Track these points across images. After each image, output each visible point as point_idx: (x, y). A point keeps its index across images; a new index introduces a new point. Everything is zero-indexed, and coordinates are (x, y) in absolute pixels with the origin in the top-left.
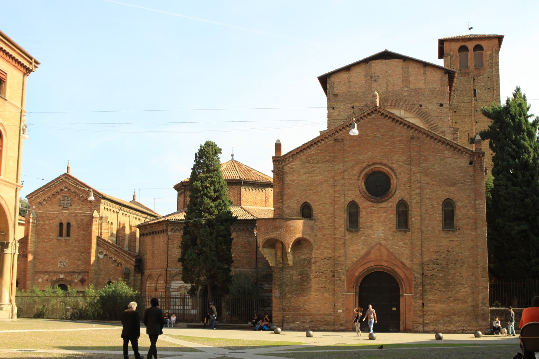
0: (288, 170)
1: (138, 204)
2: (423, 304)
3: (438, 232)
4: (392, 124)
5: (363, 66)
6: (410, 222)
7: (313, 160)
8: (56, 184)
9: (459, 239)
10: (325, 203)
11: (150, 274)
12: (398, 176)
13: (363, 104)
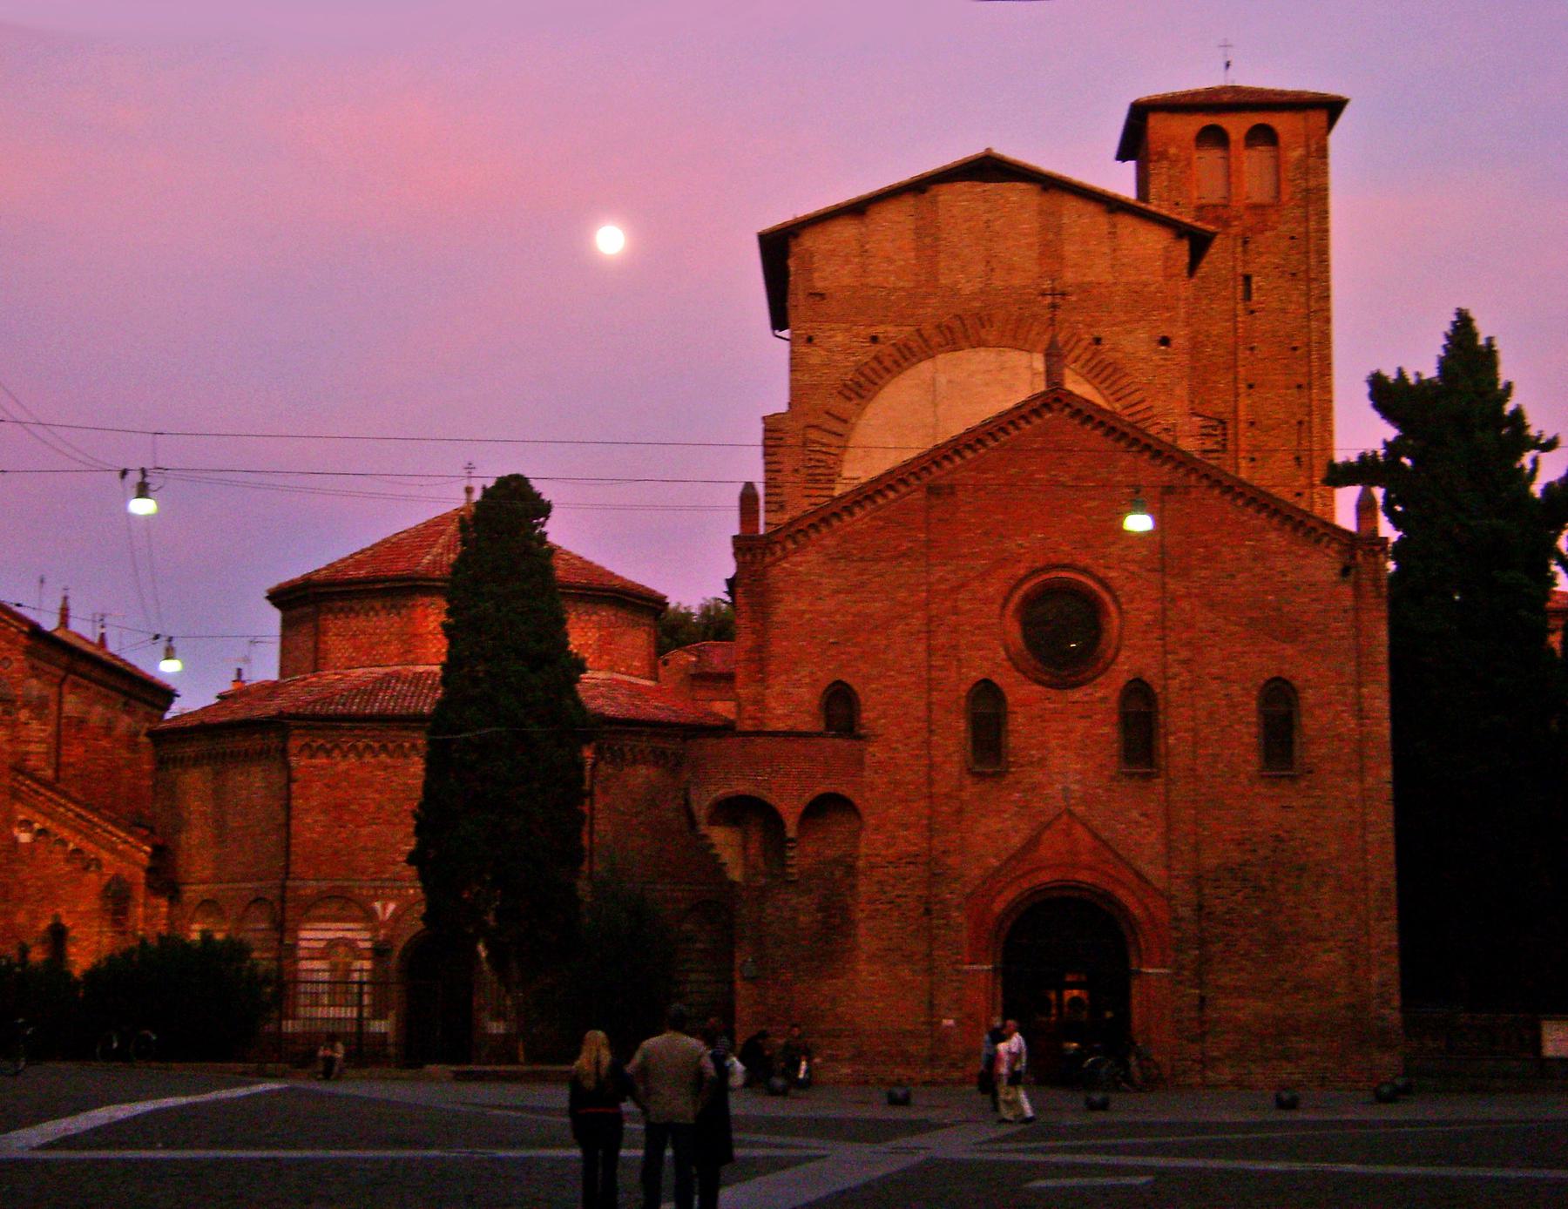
0: (783, 580)
3: (1246, 782)
6: (1163, 751)
9: (1312, 801)
12: (1124, 607)
13: (908, 328)
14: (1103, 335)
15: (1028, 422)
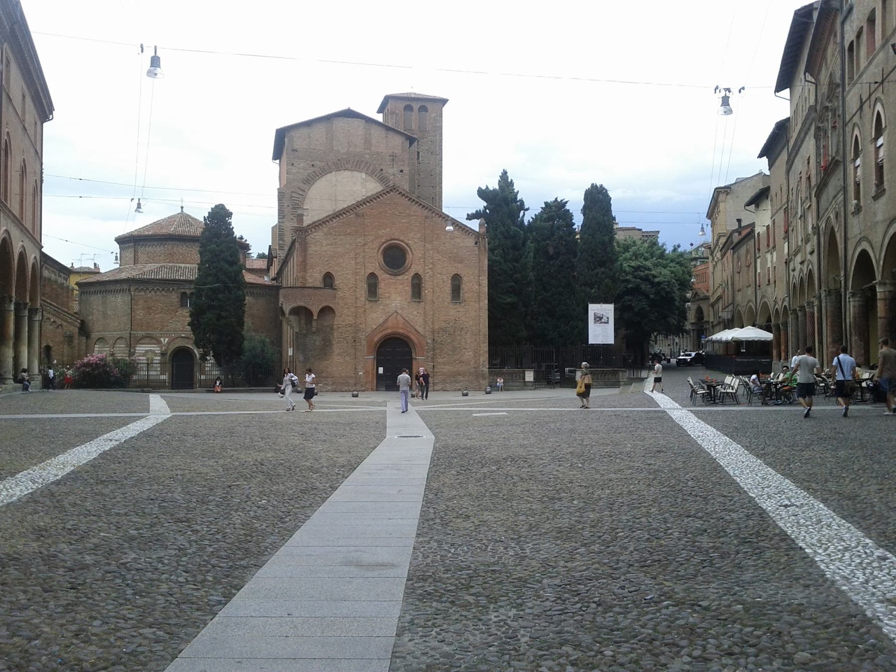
4: (409, 203)
7: (335, 232)
10: (347, 274)
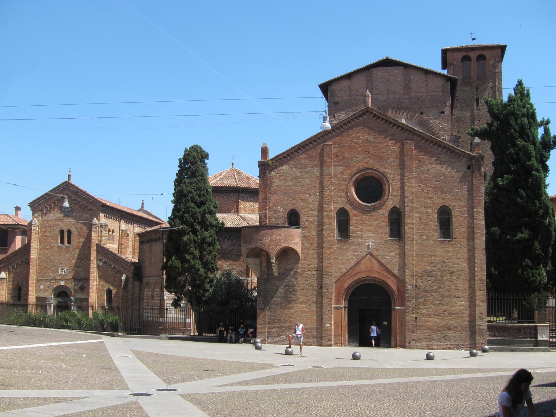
1: (146, 212)
2: (416, 318)
5: (364, 74)
6: (403, 231)
8: (57, 192)
9: (456, 249)
11: (147, 282)
14: (423, 111)
15: (358, 119)
